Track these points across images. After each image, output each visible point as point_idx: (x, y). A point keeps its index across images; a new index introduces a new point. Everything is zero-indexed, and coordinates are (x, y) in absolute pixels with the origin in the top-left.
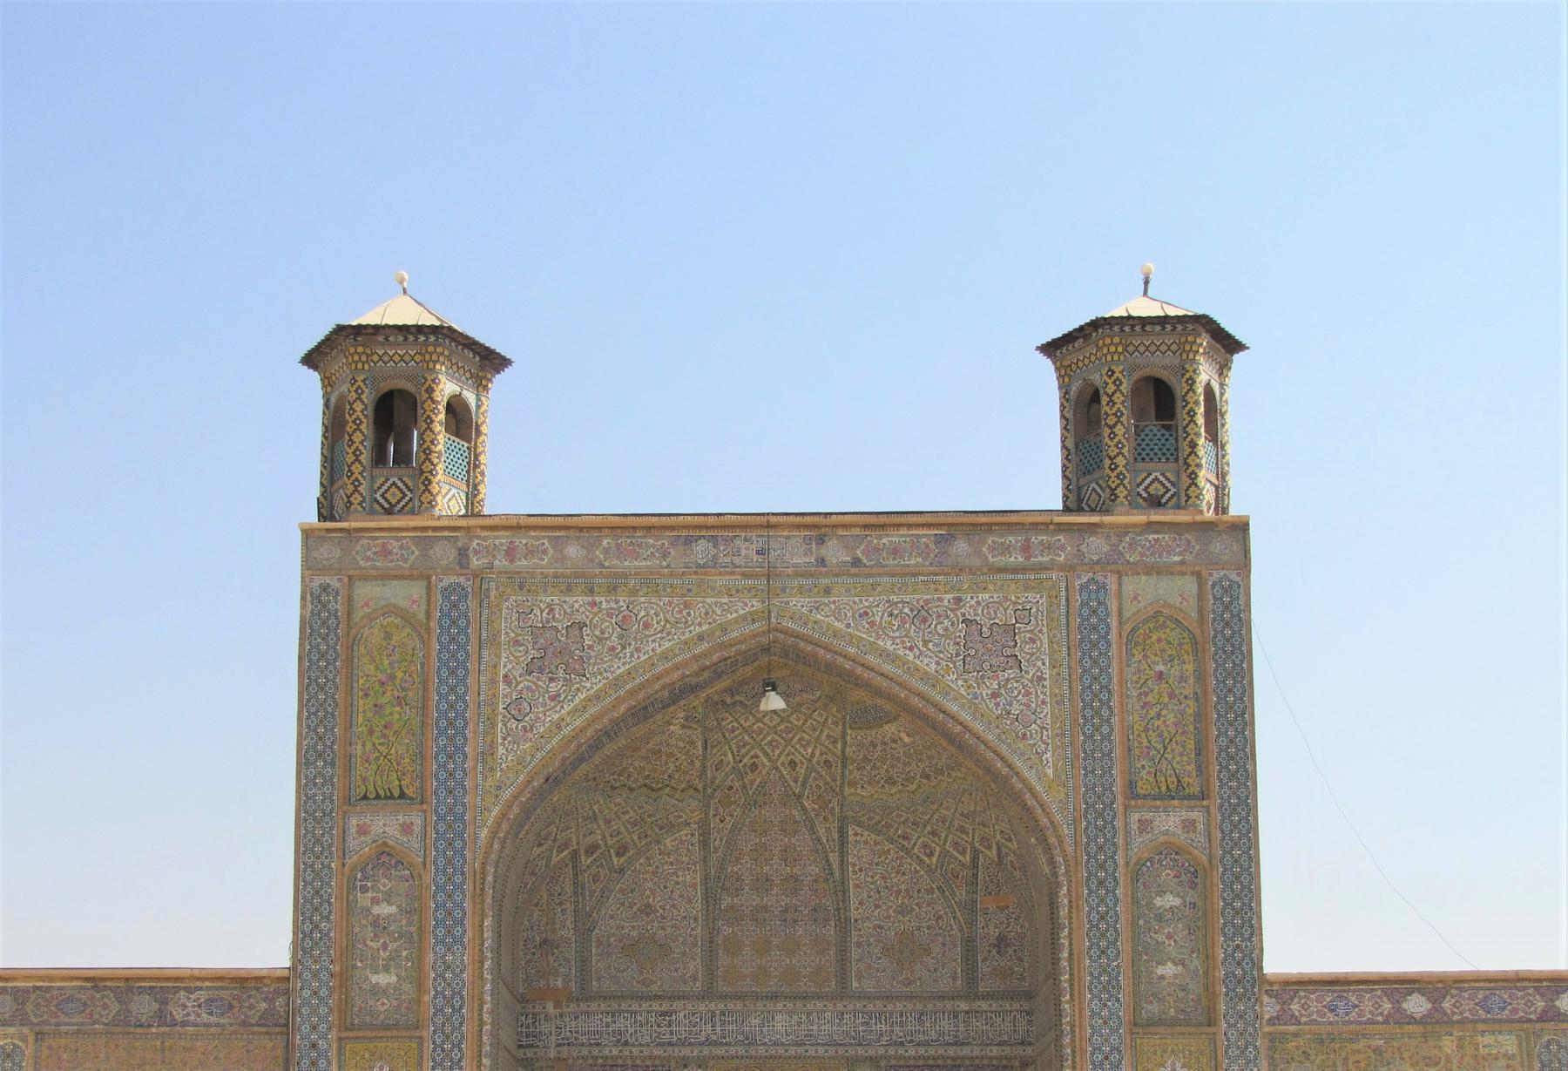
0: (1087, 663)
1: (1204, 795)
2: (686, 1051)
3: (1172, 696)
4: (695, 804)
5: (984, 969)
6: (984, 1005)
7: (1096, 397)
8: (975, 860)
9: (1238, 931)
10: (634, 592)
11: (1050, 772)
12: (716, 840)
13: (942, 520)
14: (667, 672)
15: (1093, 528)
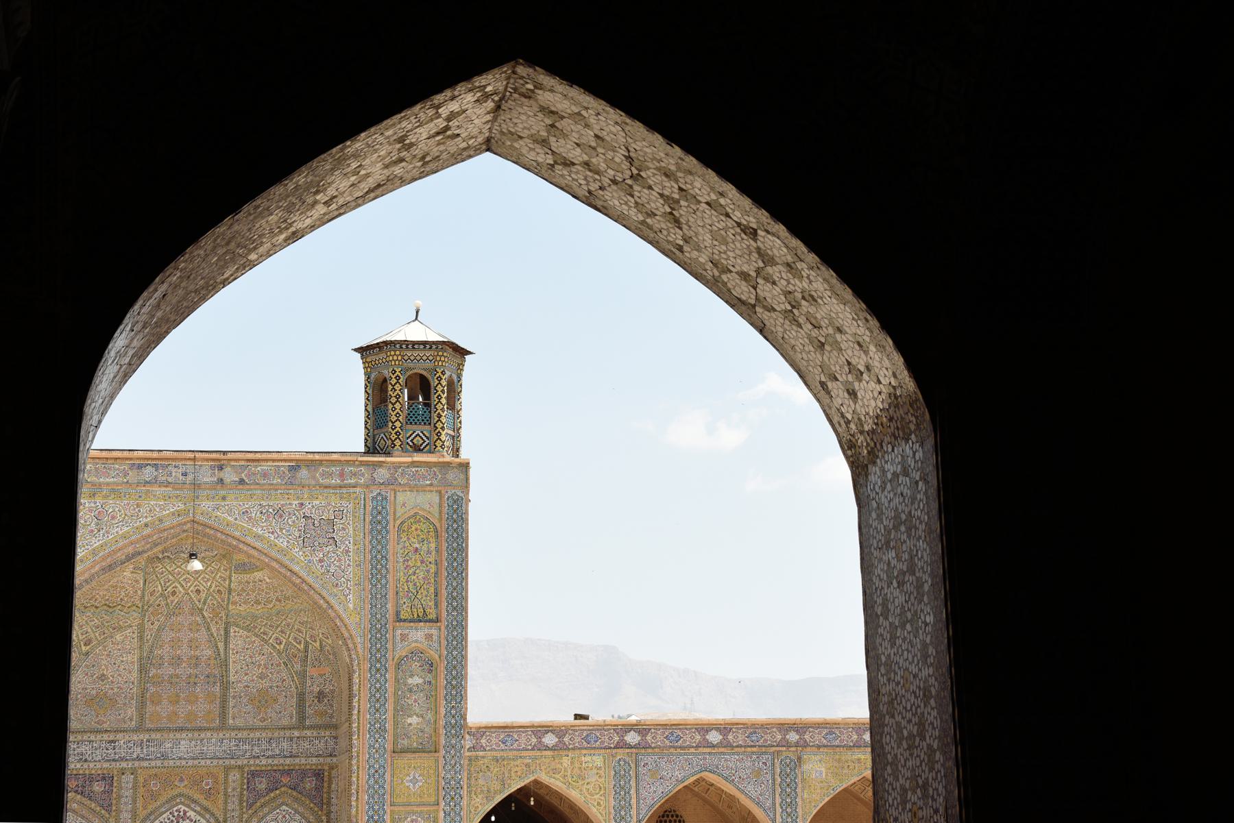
0: (375, 542)
1: (437, 620)
2: (124, 765)
3: (422, 562)
4: (136, 615)
5: (309, 711)
6: (309, 733)
7: (385, 380)
8: (306, 647)
9: (454, 698)
10: (106, 497)
11: (351, 606)
12: (148, 635)
13: (293, 457)
14: (125, 546)
15: (380, 464)
